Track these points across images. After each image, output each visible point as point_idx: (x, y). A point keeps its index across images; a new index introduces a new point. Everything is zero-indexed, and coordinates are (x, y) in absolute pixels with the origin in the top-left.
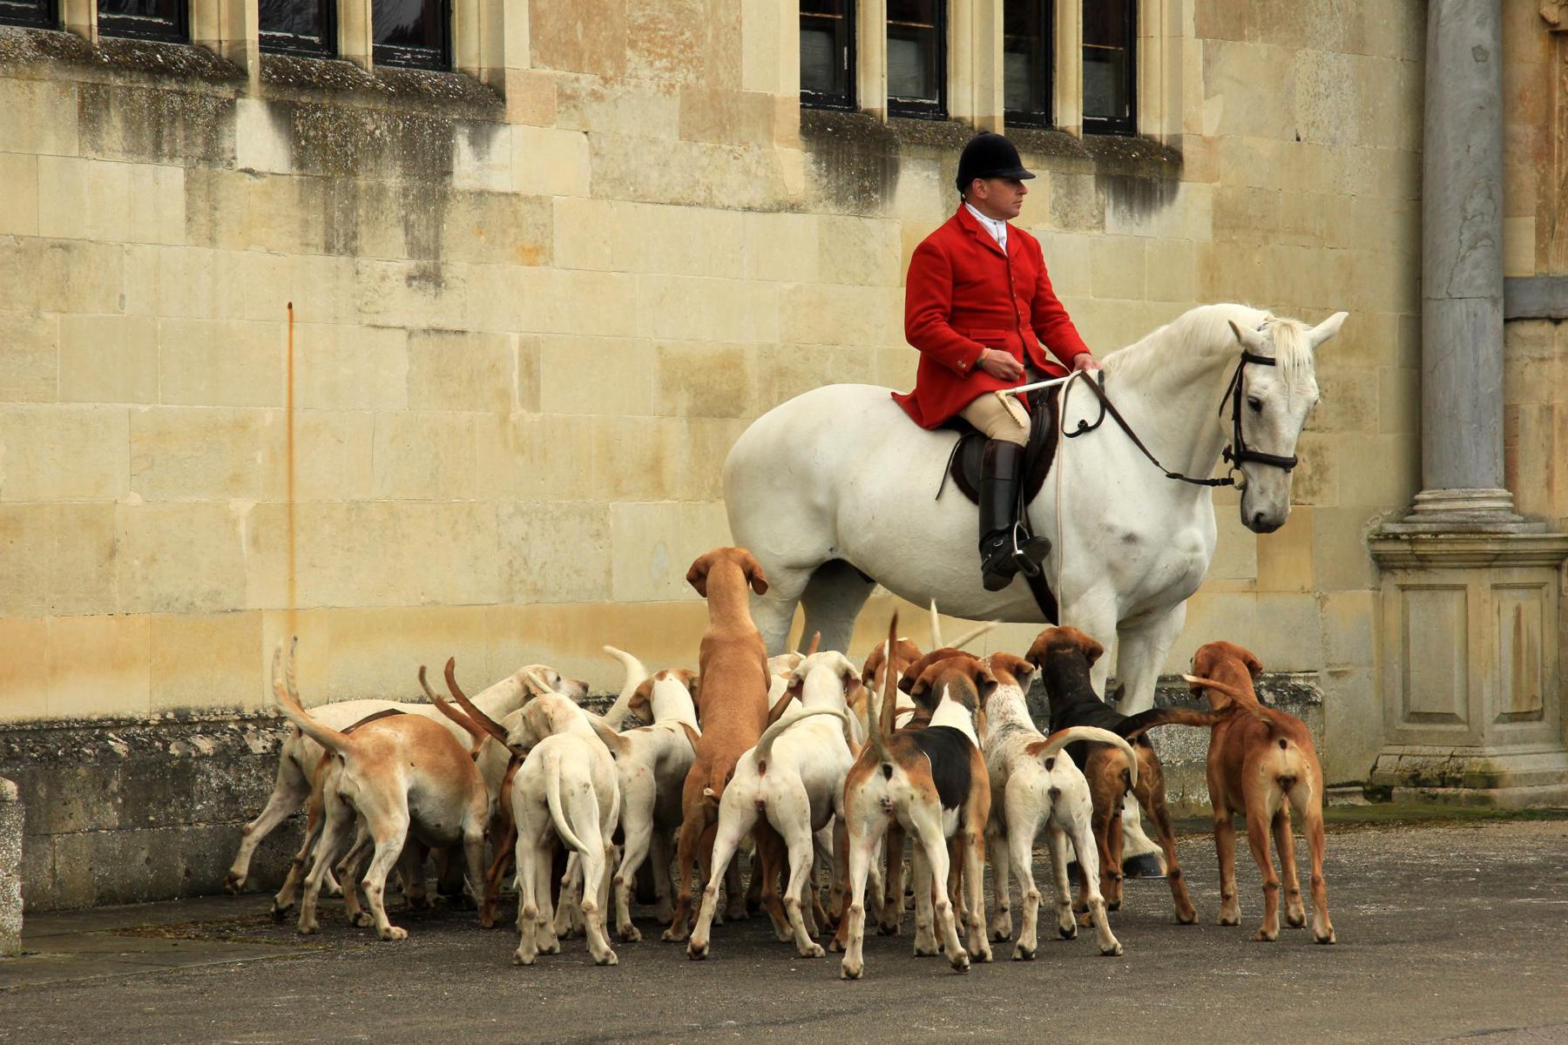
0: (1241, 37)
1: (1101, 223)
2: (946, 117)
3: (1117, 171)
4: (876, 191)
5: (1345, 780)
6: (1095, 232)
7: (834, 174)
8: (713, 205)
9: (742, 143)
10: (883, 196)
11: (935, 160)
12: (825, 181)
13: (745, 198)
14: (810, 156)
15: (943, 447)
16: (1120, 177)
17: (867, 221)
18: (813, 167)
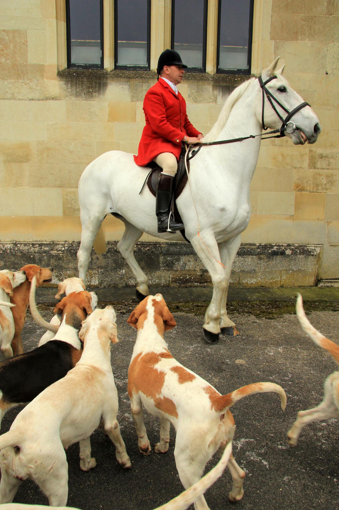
0: (297, 39)
1: (215, 101)
2: (150, 70)
3: (225, 84)
4: (95, 92)
5: (334, 278)
6: (211, 104)
7: (75, 88)
8: (14, 99)
9: (28, 79)
10: (99, 94)
11: (127, 82)
12: (70, 90)
13: (30, 97)
14: (62, 83)
15: (146, 173)
16: (225, 86)
17: (91, 102)
18: (64, 86)
